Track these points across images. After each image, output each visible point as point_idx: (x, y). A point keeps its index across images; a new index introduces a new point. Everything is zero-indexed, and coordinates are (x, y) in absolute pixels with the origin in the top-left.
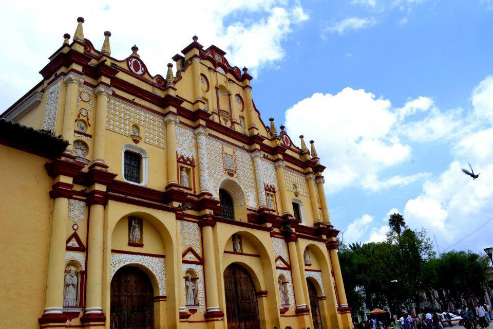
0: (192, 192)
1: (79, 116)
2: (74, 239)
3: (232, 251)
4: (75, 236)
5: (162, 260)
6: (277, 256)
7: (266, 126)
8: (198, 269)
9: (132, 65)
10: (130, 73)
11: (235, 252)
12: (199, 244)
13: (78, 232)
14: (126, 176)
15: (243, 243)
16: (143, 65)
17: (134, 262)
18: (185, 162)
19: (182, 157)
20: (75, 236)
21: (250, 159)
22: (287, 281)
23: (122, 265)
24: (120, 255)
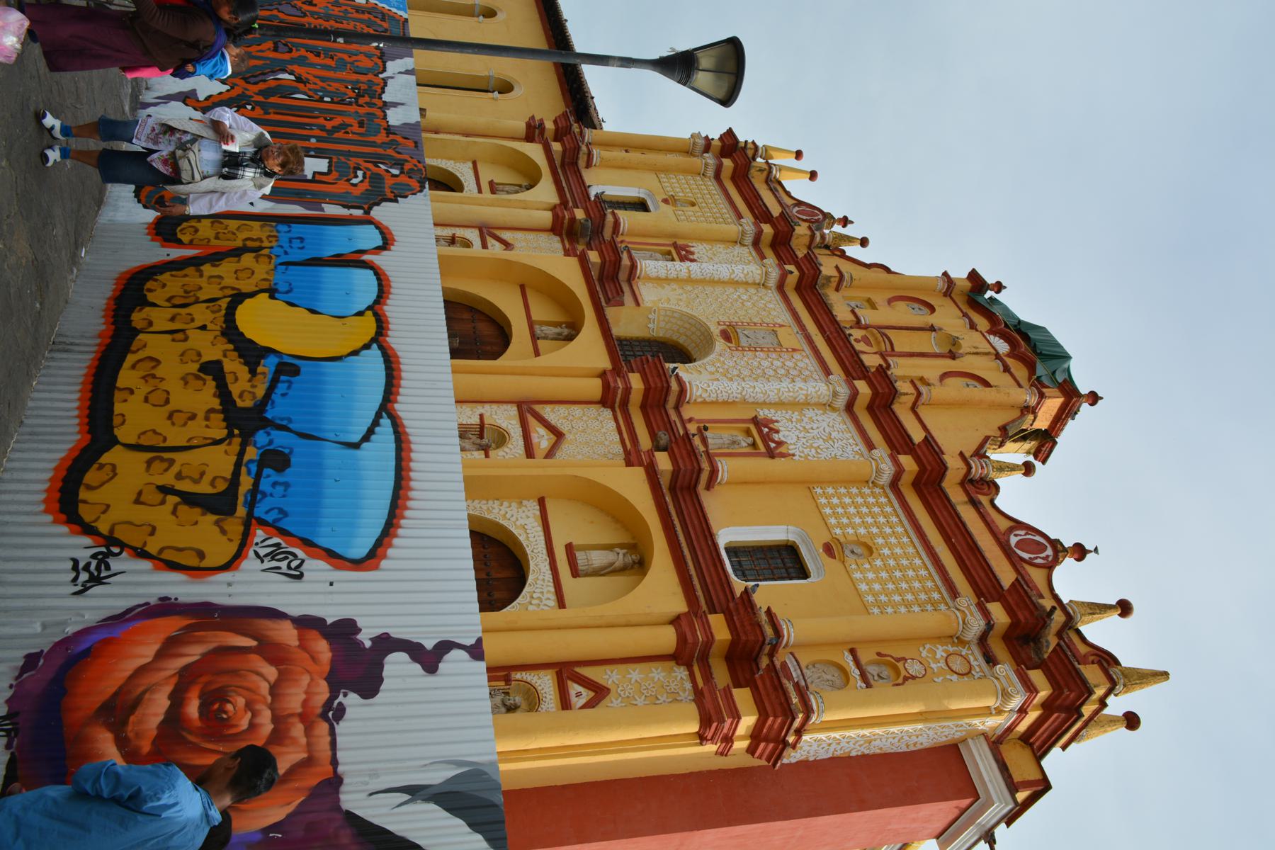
3: (534, 317)
11: (531, 324)
23: (459, 175)
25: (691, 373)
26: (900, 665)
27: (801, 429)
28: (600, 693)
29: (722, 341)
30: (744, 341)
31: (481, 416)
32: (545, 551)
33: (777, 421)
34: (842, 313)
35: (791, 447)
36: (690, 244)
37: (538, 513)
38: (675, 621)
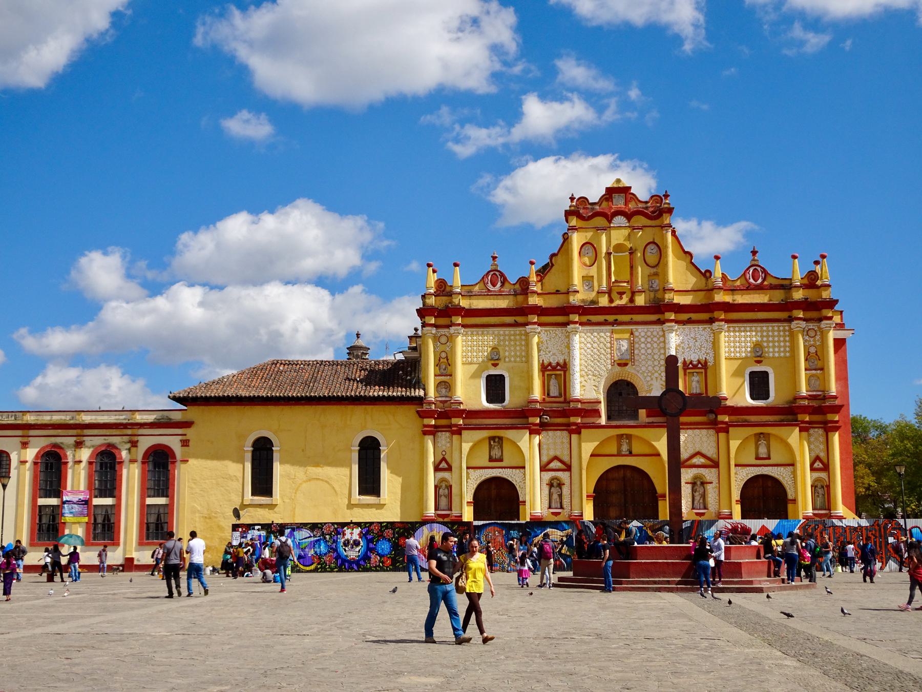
0: (562, 399)
1: (440, 360)
2: (443, 462)
3: (615, 453)
4: (444, 459)
5: (522, 470)
6: (697, 450)
7: (703, 271)
8: (564, 476)
9: (489, 282)
10: (488, 294)
11: (619, 454)
12: (567, 452)
13: (446, 456)
14: (489, 400)
15: (633, 442)
16: (502, 275)
17: (494, 475)
18: (554, 369)
19: (550, 364)
20: (444, 459)
21: (661, 333)
22: (708, 481)
23: (483, 478)
24: (481, 470)
25: (652, 389)
26: (811, 354)
27: (689, 349)
28: (817, 458)
29: (627, 367)
30: (629, 357)
31: (686, 483)
32: (759, 468)
33: (684, 359)
34: (604, 302)
35: (701, 358)
36: (541, 362)
37: (740, 468)
38: (800, 431)
